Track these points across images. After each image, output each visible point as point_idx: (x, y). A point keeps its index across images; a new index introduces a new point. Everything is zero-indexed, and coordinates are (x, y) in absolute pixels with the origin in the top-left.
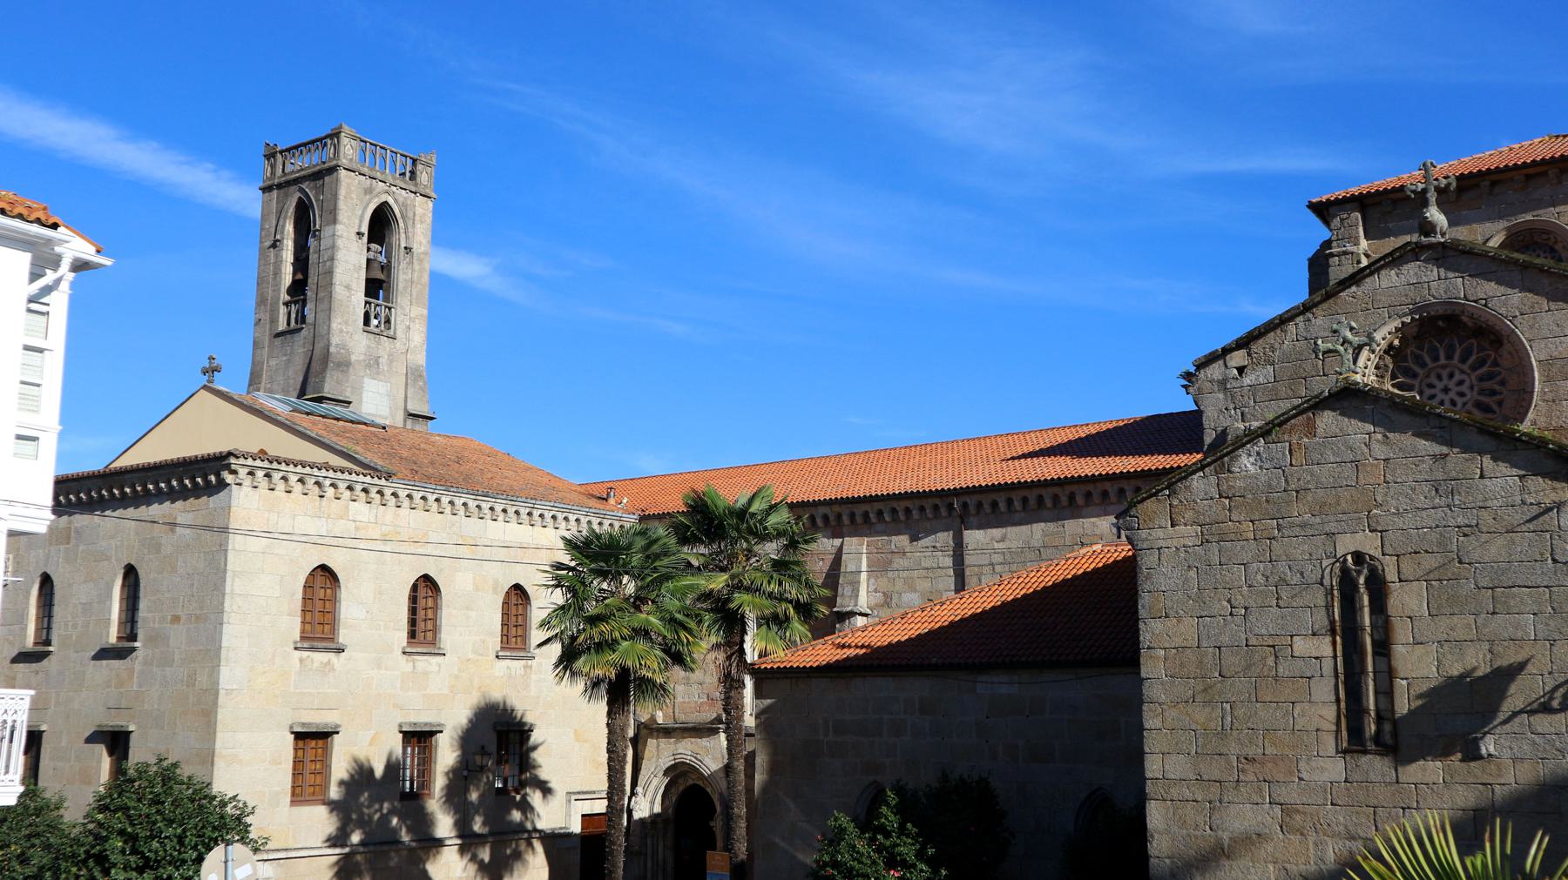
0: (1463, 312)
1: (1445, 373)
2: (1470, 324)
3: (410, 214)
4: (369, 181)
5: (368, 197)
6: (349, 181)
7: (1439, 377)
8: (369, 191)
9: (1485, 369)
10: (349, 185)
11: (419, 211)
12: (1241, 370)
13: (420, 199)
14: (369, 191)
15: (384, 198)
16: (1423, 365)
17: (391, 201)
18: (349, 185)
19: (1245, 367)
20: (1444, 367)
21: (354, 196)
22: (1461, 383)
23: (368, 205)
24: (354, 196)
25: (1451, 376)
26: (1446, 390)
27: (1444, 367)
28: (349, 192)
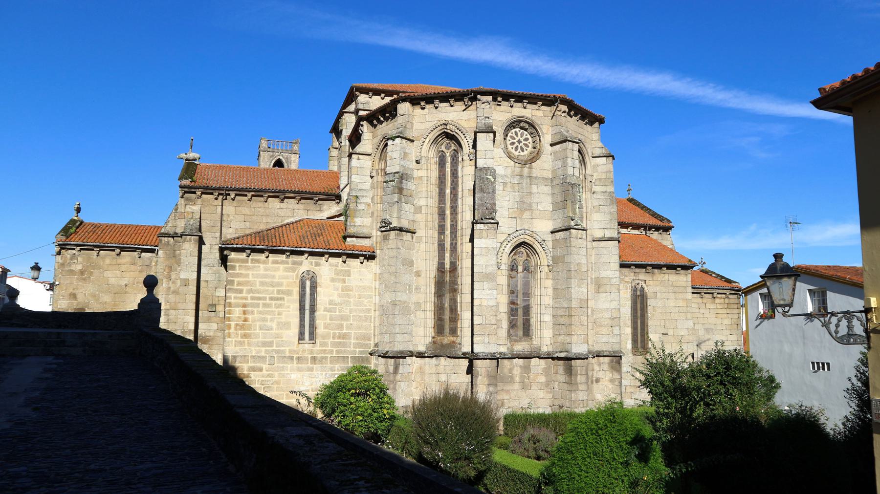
3: (290, 161)
4: (272, 153)
5: (272, 158)
6: (264, 154)
8: (271, 157)
10: (264, 156)
11: (293, 159)
13: (293, 155)
14: (272, 156)
15: (278, 158)
17: (281, 158)
18: (264, 156)
21: (266, 159)
23: (272, 160)
24: (266, 159)
28: (264, 158)
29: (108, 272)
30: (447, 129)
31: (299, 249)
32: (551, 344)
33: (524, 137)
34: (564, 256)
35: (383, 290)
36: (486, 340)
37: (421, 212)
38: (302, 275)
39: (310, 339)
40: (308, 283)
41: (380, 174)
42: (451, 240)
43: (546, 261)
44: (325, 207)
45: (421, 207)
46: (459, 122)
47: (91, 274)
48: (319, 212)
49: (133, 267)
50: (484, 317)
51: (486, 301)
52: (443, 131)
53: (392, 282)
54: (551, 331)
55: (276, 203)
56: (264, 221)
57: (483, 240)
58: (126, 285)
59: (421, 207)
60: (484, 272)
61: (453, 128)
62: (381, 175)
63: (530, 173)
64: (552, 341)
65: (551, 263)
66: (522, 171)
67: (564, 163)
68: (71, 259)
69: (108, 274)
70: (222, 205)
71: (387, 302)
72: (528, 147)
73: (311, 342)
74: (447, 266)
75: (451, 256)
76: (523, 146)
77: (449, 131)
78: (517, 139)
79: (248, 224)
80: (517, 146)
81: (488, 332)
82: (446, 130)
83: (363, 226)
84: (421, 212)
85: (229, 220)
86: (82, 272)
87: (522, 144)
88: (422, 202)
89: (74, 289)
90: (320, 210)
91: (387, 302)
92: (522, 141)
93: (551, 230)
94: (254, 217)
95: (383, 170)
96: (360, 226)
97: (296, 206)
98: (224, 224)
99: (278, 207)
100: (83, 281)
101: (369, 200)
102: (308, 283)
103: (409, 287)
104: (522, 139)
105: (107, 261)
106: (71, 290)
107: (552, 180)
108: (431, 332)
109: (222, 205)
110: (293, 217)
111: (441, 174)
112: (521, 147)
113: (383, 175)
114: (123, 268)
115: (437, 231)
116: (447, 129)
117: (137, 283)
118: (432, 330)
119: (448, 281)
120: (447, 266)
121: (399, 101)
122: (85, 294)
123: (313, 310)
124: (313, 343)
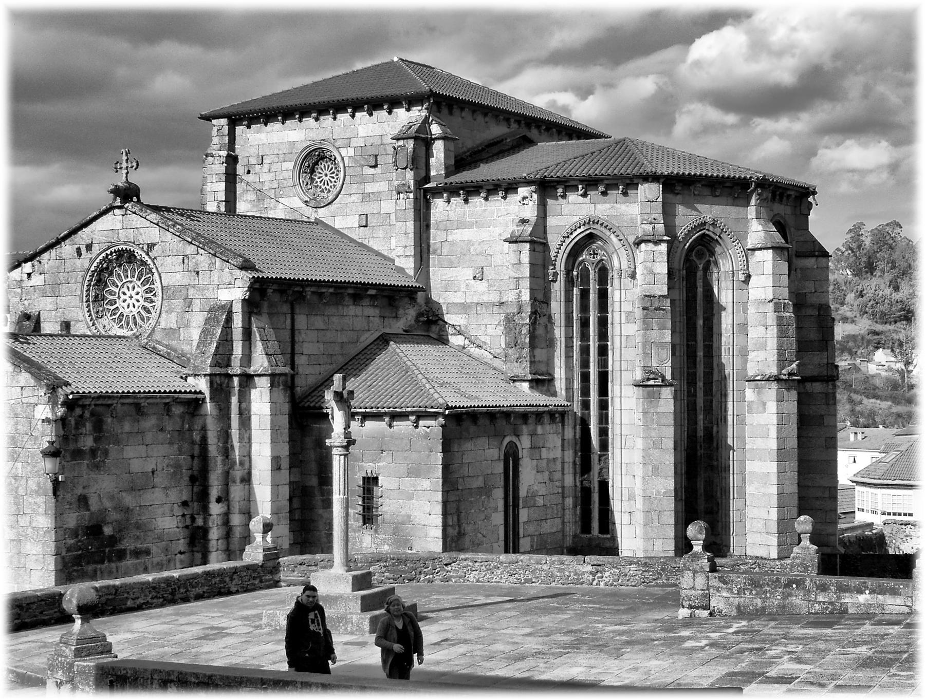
0: (134, 251)
1: (130, 286)
2: (138, 257)
7: (128, 288)
9: (147, 286)
12: (29, 275)
16: (121, 280)
19: (31, 273)
20: (131, 282)
22: (138, 293)
25: (134, 288)
26: (131, 297)
27: (131, 282)
29: (128, 448)
35: (650, 474)
44: (401, 312)
47: (106, 453)
48: (395, 320)
49: (161, 436)
56: (340, 341)
58: (153, 472)
68: (77, 428)
69: (130, 452)
70: (293, 314)
71: (658, 492)
74: (700, 433)
75: (705, 419)
79: (321, 346)
82: (707, 232)
85: (301, 340)
86: (93, 452)
89: (84, 488)
91: (658, 492)
94: (328, 334)
98: (296, 347)
100: (95, 469)
105: (127, 427)
106: (79, 491)
109: (293, 314)
111: (690, 295)
114: (149, 437)
117: (167, 466)
120: (700, 433)
122: (99, 495)
123: (516, 506)
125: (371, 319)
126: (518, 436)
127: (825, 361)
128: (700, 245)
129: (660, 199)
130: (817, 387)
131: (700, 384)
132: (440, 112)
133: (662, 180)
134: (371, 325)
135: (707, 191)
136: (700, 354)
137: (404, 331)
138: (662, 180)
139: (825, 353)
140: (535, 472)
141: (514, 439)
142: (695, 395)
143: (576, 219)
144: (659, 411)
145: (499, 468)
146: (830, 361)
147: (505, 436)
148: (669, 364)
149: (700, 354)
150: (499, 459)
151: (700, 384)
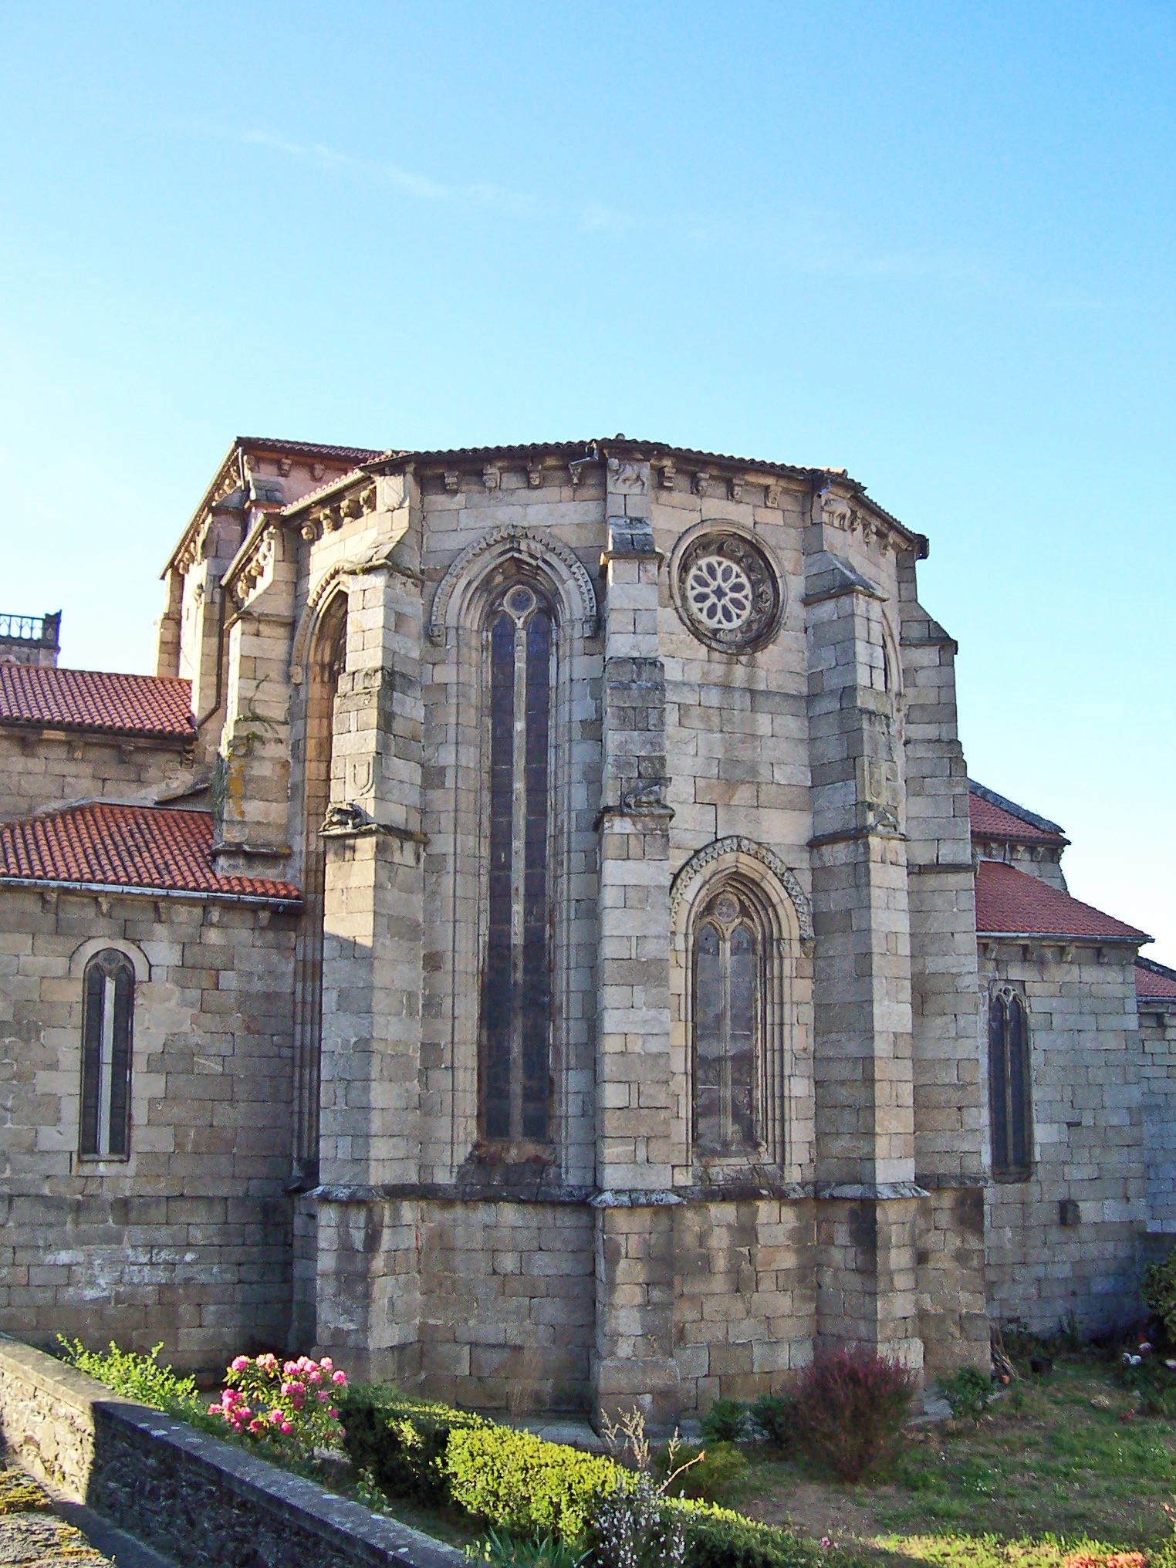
30: (520, 551)
31: (85, 885)
32: (812, 1161)
33: (733, 580)
34: (849, 912)
35: (334, 1008)
36: (641, 1154)
37: (444, 783)
38: (93, 963)
39: (113, 1149)
40: (110, 987)
41: (318, 679)
42: (527, 867)
43: (795, 924)
44: (152, 773)
45: (442, 771)
46: (556, 531)
48: (134, 786)
50: (634, 1087)
51: (640, 1042)
52: (509, 555)
53: (361, 985)
54: (811, 1124)
55: (14, 759)
57: (629, 863)
59: (442, 771)
60: (634, 956)
61: (537, 548)
62: (322, 681)
63: (751, 678)
64: (813, 1151)
65: (810, 932)
66: (728, 674)
67: (845, 652)
72: (743, 608)
73: (116, 1157)
74: (517, 938)
75: (528, 912)
76: (730, 607)
77: (525, 557)
78: (714, 585)
80: (714, 605)
81: (644, 1131)
82: (516, 555)
83: (269, 824)
84: (442, 786)
87: (725, 601)
88: (446, 757)
90: (140, 781)
92: (727, 590)
93: (803, 842)
95: (327, 668)
96: (259, 823)
97: (69, 768)
99: (20, 767)
101: (283, 752)
102: (110, 987)
103: (408, 999)
104: (726, 587)
107: (811, 698)
108: (469, 1130)
110: (62, 797)
112: (724, 607)
113: (326, 680)
115: (488, 840)
116: (520, 551)
118: (472, 1124)
119: (520, 981)
120: (517, 938)
121: (384, 469)
124: (121, 1161)
125: (69, 779)
126: (136, 942)
127: (852, 799)
128: (520, 582)
129: (407, 504)
130: (838, 854)
131: (518, 844)
132: (285, 476)
133: (410, 468)
134: (67, 790)
135: (512, 481)
136: (519, 786)
137: (157, 803)
138: (410, 468)
139: (852, 783)
140: (195, 1011)
141: (122, 945)
142: (508, 866)
143: (325, 570)
144: (354, 882)
145: (74, 992)
146: (860, 799)
147: (90, 938)
148: (372, 793)
149: (519, 786)
150: (69, 975)
151: (518, 844)
